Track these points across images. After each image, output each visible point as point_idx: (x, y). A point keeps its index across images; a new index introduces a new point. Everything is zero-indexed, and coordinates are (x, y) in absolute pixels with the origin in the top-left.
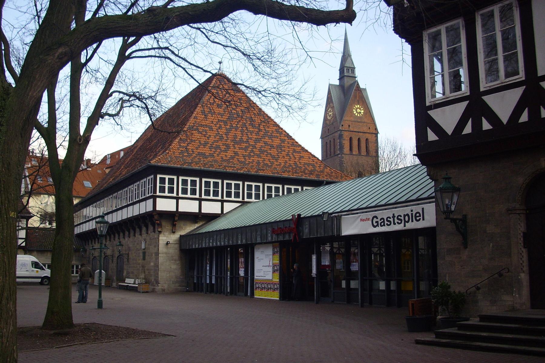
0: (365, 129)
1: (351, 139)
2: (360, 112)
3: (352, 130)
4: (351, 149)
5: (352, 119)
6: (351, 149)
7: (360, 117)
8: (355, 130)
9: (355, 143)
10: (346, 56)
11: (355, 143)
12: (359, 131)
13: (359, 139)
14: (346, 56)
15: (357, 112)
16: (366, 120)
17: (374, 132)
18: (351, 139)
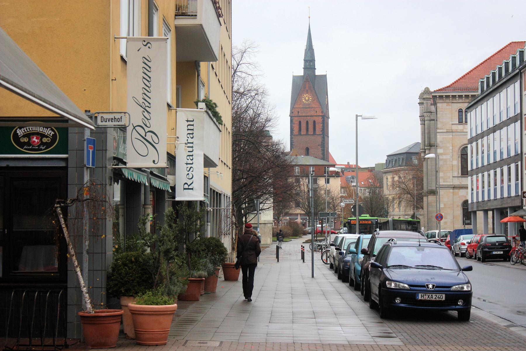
0: (312, 113)
1: (300, 122)
2: (308, 100)
3: (300, 114)
4: (300, 130)
5: (301, 106)
6: (300, 130)
7: (309, 104)
8: (304, 115)
9: (304, 125)
10: (310, 51)
11: (304, 125)
12: (307, 115)
13: (307, 122)
14: (310, 51)
15: (305, 100)
16: (313, 106)
17: (321, 114)
18: (300, 122)
